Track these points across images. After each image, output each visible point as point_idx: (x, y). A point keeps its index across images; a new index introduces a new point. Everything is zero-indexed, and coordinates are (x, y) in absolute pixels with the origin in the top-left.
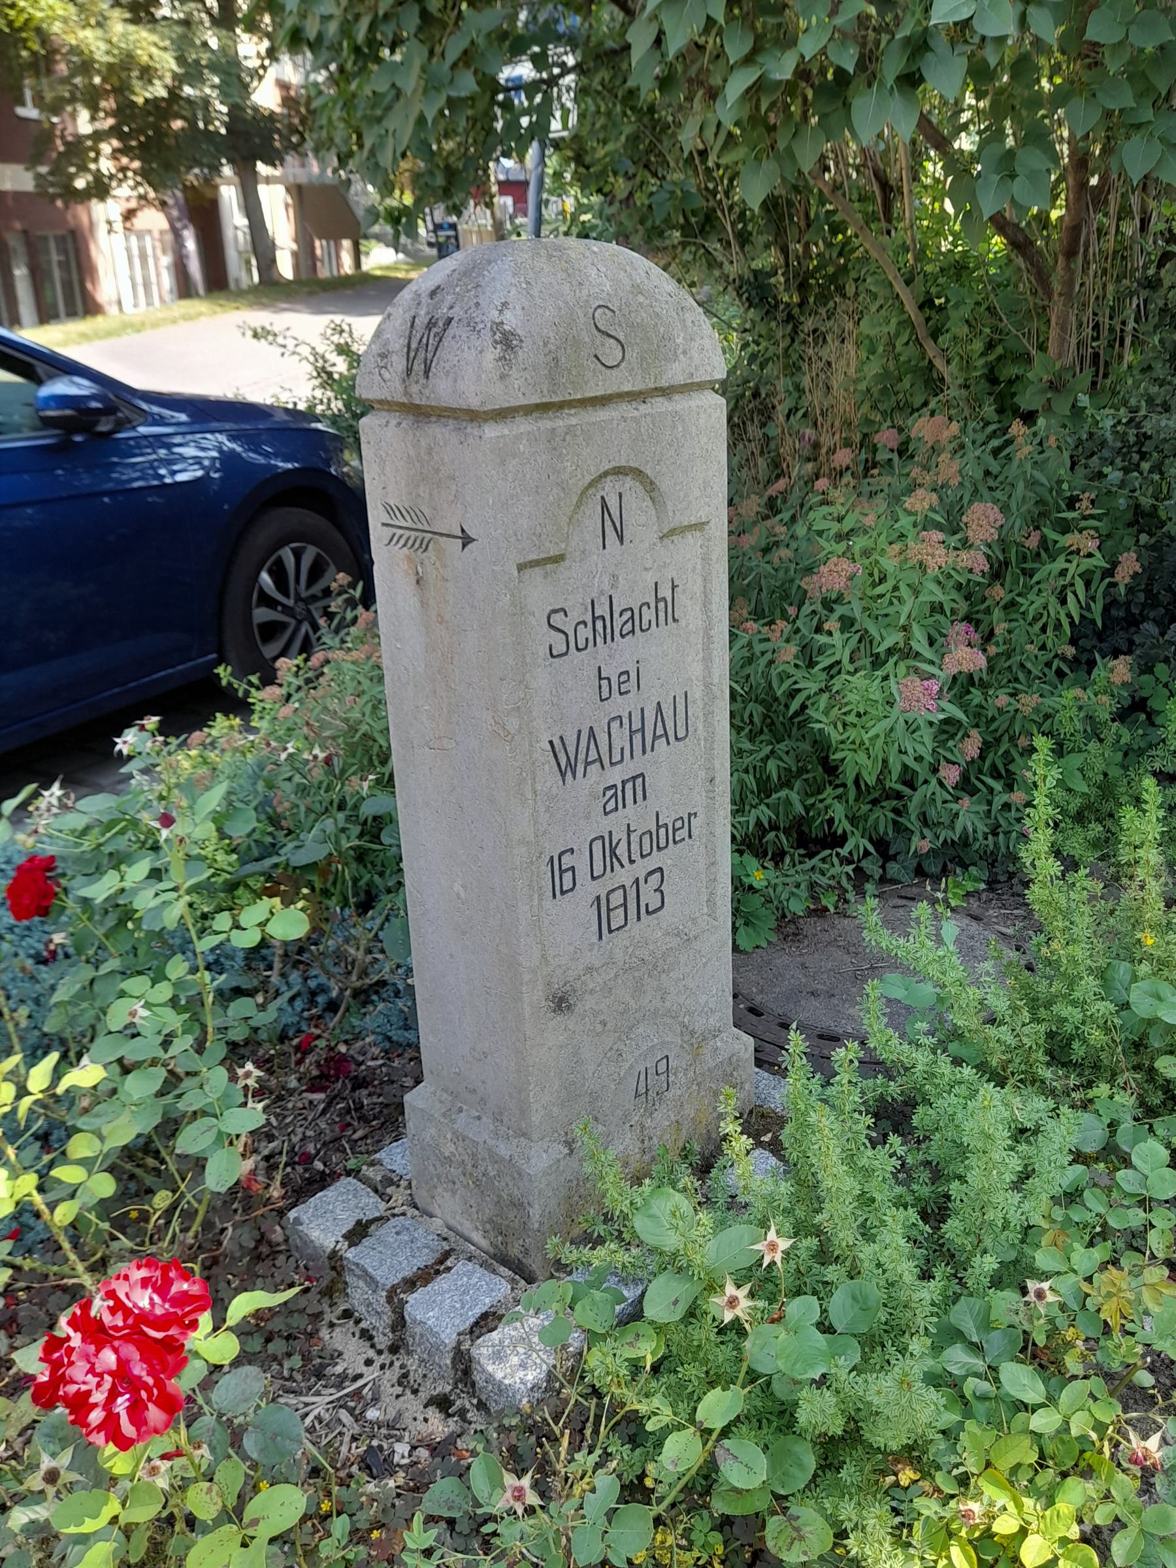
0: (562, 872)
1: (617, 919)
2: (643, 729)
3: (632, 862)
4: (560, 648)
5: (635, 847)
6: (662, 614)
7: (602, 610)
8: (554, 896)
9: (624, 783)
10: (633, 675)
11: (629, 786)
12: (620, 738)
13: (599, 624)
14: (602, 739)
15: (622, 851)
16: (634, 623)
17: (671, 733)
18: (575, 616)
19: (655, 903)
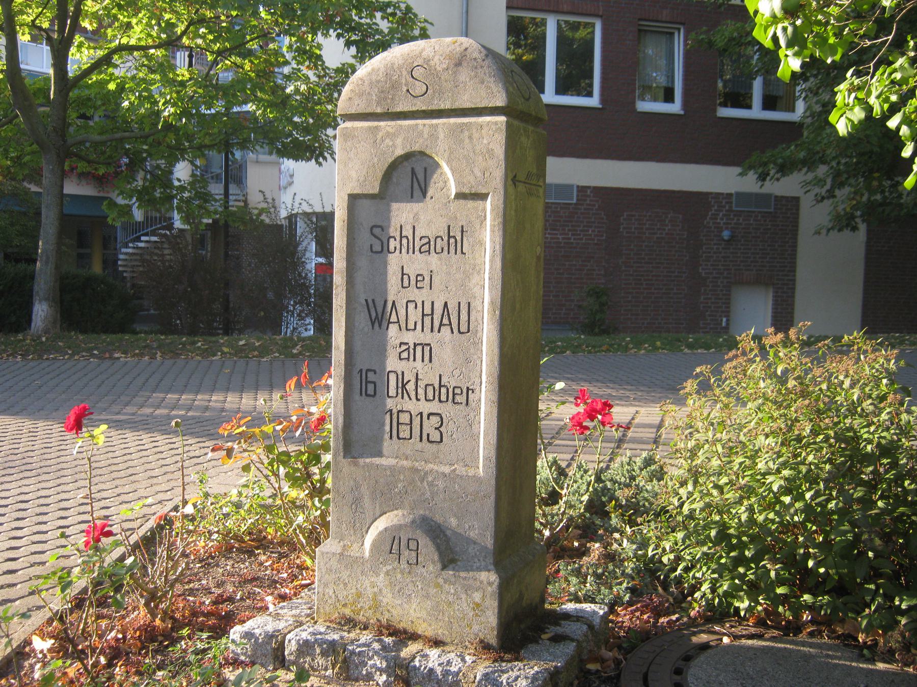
0: (367, 382)
1: (405, 432)
3: (418, 400)
4: (377, 248)
5: (421, 391)
7: (407, 232)
8: (361, 394)
10: (427, 279)
11: (419, 349)
12: (415, 316)
14: (402, 312)
15: (411, 387)
17: (455, 326)
19: (435, 436)
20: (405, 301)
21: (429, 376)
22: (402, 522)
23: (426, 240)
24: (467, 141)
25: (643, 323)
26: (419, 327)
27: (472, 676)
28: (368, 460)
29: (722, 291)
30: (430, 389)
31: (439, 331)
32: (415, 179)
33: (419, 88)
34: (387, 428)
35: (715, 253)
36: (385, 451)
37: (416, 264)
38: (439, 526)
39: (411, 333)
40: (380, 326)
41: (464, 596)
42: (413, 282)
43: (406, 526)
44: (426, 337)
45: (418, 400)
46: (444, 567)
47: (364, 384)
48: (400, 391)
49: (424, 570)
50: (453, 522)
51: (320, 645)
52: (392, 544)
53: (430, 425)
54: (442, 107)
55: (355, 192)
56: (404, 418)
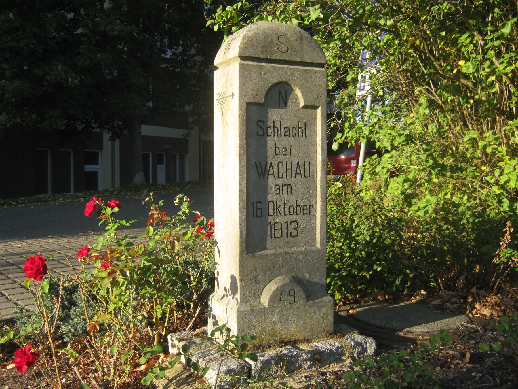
0: (257, 209)
1: (278, 234)
3: (285, 215)
4: (261, 133)
6: (300, 133)
7: (277, 124)
8: (254, 216)
9: (283, 186)
11: (285, 187)
12: (282, 170)
14: (276, 168)
15: (281, 209)
17: (303, 174)
19: (294, 233)
20: (277, 162)
21: (290, 201)
22: (285, 282)
23: (287, 129)
24: (309, 79)
26: (285, 175)
27: (350, 345)
28: (260, 253)
30: (291, 209)
32: (281, 97)
33: (284, 49)
34: (269, 233)
36: (268, 247)
37: (283, 142)
38: (300, 279)
39: (281, 179)
41: (318, 312)
43: (288, 283)
44: (288, 181)
45: (285, 215)
46: (308, 301)
47: (255, 210)
48: (275, 211)
49: (298, 305)
50: (307, 276)
51: (274, 360)
52: (279, 297)
53: (291, 228)
54: (296, 60)
55: (250, 101)
56: (278, 226)
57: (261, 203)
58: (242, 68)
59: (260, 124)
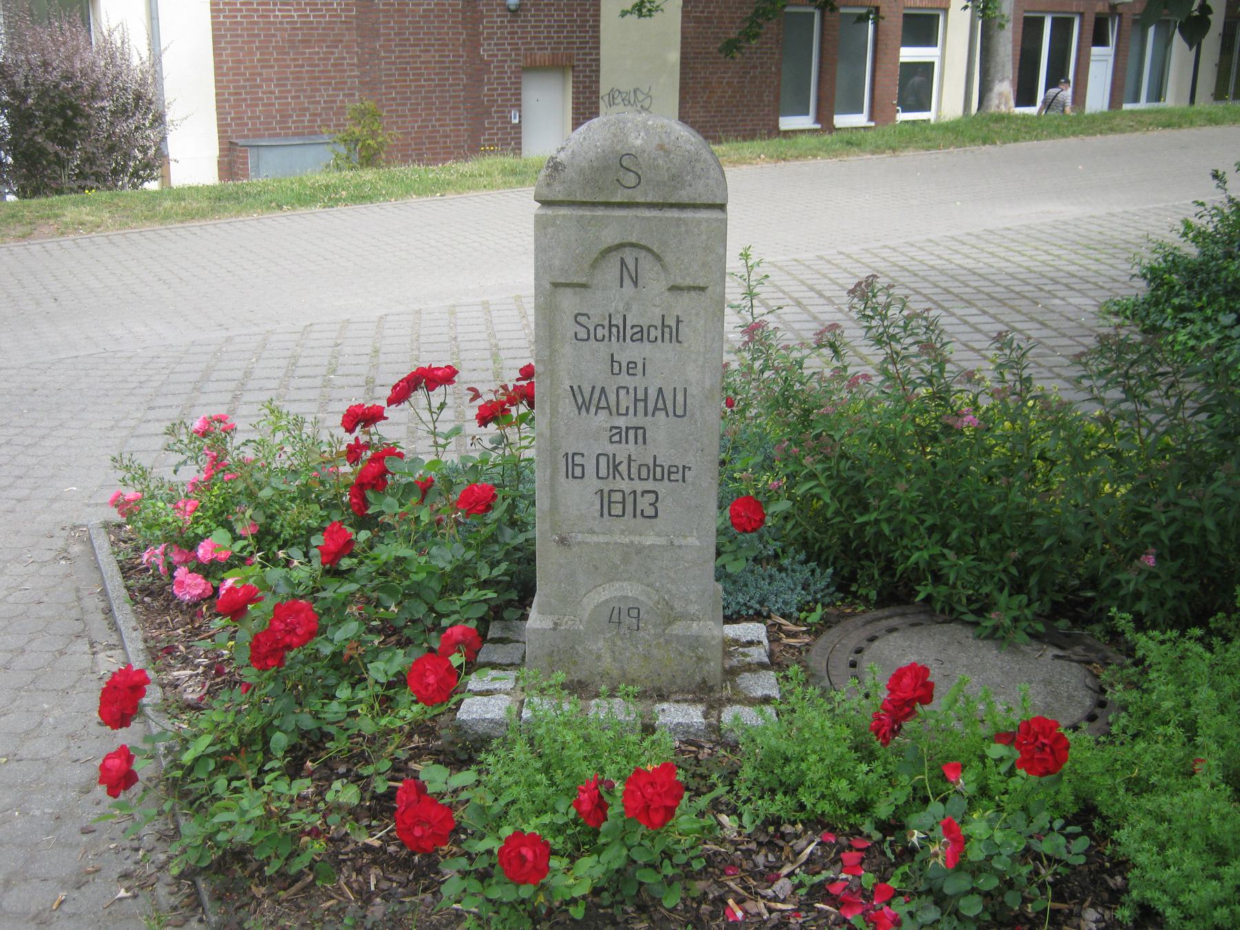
0: (574, 465)
1: (617, 509)
2: (645, 400)
5: (634, 470)
6: (667, 336)
7: (617, 320)
10: (640, 366)
11: (631, 432)
13: (614, 330)
14: (612, 398)
15: (623, 468)
16: (641, 335)
18: (596, 320)
19: (650, 511)
21: (643, 455)
25: (413, 127)
26: (631, 411)
29: (509, 78)
31: (653, 415)
35: (499, 28)
40: (588, 410)
42: (624, 369)
44: (639, 421)
53: (644, 503)
56: (617, 497)
57: (583, 455)
58: (541, 224)
59: (581, 319)
